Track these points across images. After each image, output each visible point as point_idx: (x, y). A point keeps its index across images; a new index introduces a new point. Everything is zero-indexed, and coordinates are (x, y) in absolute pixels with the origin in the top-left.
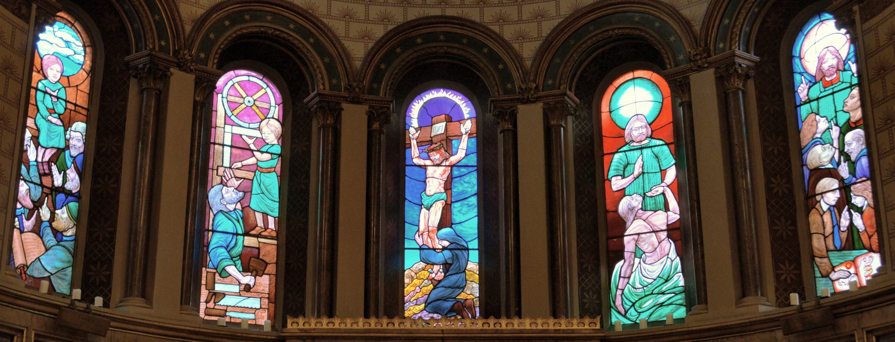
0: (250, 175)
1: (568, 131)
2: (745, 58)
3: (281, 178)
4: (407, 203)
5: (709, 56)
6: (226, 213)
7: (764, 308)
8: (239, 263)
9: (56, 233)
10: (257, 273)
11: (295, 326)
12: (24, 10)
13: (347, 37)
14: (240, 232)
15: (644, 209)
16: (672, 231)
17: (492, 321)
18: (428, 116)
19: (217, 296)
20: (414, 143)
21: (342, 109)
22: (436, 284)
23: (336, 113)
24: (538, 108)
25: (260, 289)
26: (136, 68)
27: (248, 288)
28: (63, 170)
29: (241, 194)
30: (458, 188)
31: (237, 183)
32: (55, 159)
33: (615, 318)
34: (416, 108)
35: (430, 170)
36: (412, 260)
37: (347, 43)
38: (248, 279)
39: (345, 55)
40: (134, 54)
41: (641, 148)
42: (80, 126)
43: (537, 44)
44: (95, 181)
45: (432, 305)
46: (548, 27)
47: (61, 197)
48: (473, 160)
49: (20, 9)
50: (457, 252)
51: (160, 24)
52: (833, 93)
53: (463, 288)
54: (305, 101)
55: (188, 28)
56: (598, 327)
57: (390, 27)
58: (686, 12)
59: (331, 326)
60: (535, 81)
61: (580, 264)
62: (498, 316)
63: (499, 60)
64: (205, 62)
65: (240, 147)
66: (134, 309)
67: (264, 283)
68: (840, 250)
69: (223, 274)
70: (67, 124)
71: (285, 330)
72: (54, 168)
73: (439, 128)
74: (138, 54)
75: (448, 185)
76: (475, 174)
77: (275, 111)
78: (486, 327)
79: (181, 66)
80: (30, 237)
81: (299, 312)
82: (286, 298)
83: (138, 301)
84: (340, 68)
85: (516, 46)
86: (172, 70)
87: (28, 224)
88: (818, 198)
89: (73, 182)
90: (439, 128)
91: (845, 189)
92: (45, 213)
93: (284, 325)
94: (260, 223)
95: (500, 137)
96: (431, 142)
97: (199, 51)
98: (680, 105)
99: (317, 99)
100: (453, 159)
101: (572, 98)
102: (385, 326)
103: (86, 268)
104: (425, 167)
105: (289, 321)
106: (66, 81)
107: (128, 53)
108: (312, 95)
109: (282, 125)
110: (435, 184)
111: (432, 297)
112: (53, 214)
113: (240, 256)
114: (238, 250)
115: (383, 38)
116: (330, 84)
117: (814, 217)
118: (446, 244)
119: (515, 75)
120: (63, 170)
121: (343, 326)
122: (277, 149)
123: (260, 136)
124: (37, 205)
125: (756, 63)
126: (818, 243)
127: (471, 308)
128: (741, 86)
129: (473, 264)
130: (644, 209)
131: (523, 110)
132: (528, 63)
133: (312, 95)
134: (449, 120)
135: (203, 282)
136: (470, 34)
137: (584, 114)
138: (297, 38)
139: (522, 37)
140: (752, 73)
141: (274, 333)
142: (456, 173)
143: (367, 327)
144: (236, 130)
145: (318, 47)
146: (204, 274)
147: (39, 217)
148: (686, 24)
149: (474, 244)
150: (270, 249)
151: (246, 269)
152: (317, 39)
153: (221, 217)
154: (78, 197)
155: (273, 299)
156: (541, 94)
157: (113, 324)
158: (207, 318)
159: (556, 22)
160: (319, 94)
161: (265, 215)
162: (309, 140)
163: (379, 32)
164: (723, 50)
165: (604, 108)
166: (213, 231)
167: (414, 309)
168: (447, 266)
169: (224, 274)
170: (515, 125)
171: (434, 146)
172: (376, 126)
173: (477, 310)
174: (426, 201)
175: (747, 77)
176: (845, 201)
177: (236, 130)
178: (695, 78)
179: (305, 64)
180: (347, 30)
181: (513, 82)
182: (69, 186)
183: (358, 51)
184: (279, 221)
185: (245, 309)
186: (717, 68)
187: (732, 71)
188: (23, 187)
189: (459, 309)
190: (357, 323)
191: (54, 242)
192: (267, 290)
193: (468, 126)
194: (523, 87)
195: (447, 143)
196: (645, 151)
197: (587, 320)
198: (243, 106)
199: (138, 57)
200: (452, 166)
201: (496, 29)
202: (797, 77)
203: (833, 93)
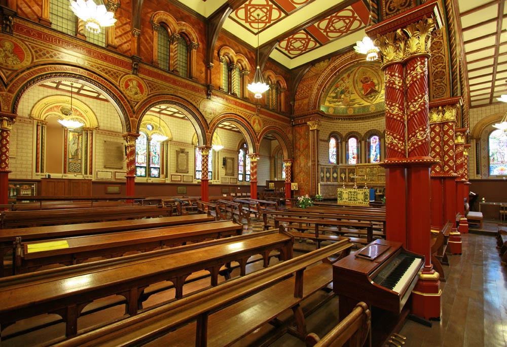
89: (335, 153)
90: (374, 141)
129: (378, 156)
193: (378, 140)
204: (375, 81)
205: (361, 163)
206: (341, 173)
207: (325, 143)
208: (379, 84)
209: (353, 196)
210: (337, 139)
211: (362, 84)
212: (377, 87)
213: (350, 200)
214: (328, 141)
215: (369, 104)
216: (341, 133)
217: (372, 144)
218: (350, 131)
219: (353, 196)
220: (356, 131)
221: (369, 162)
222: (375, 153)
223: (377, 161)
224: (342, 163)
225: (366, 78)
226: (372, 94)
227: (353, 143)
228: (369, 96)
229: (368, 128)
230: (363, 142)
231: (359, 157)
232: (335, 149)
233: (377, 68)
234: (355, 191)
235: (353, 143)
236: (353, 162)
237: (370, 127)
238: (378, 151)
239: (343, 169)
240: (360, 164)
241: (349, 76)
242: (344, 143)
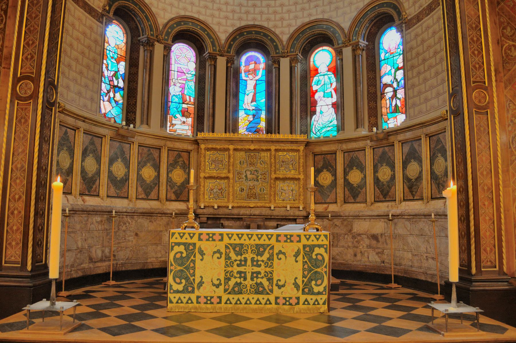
0: (184, 82)
1: (298, 68)
2: (363, 43)
3: (195, 83)
4: (240, 93)
5: (350, 42)
6: (176, 96)
7: (364, 132)
8: (181, 113)
9: (116, 102)
10: (187, 117)
11: (201, 136)
12: (101, 20)
13: (219, 32)
14: (181, 102)
15: (324, 97)
16: (334, 105)
17: (269, 135)
18: (248, 62)
19: (172, 125)
20: (243, 72)
21: (217, 58)
22: (250, 122)
23: (215, 60)
24: (288, 59)
25: (188, 123)
26: (142, 42)
27: (184, 122)
28: (117, 79)
29: (181, 89)
30: (258, 87)
31: (179, 85)
32: (114, 75)
33: (312, 135)
34: (244, 58)
35: (249, 82)
36: (241, 114)
37: (219, 34)
38: (184, 119)
39: (218, 38)
40: (141, 37)
41: (324, 75)
42: (123, 63)
43: (288, 36)
44: (129, 83)
45: (248, 129)
46: (292, 29)
47: (117, 89)
48: (264, 78)
49: (99, 19)
50: (258, 111)
51: (150, 26)
52: (393, 57)
53: (259, 124)
54: (204, 55)
55: (161, 27)
56: (306, 138)
57: (235, 28)
58: (343, 25)
59: (213, 136)
60: (287, 49)
61: (301, 116)
62: (271, 133)
63: (274, 41)
64: (167, 40)
65: (181, 72)
66: (144, 129)
67: (190, 120)
68: (392, 113)
69: (175, 117)
70: (118, 62)
71: (197, 137)
72: (114, 78)
73: (252, 66)
74: (143, 37)
75: (255, 88)
76: (264, 83)
77: (193, 59)
78: (267, 137)
79: (158, 41)
80: (107, 103)
81: (202, 131)
82: (197, 126)
83: (146, 126)
84: (216, 44)
85: (280, 36)
86: (155, 43)
87: (106, 99)
88: (385, 94)
89: (121, 84)
90: (252, 66)
91: (395, 91)
92: (112, 95)
93: (197, 135)
94: (188, 99)
95: (274, 70)
96: (249, 71)
97: (165, 35)
98: (339, 59)
99: (208, 55)
100: (257, 78)
101: (300, 56)
102: (232, 136)
103: (127, 115)
104: (246, 80)
105: (199, 134)
106: (117, 47)
107: (139, 36)
108: (206, 53)
109: (196, 64)
111: (249, 127)
112: (114, 95)
113: (181, 111)
114: (180, 109)
115: (232, 32)
116: (213, 49)
117: (383, 101)
118: (254, 108)
119: (280, 47)
120: (117, 79)
121: (217, 136)
122: (194, 73)
123: (187, 68)
124: (109, 92)
125: (367, 45)
126: (384, 110)
127: (262, 131)
128: (361, 53)
130: (324, 97)
131: (282, 60)
132: (285, 43)
133: (206, 53)
134: (256, 63)
135: (168, 120)
136: (264, 31)
137: (304, 62)
138: (201, 32)
139: (282, 33)
140: (365, 48)
141: (193, 138)
142: (258, 82)
143: (226, 136)
144: (179, 66)
145: (208, 35)
146: (168, 117)
147: (109, 96)
148: (342, 29)
149: (264, 108)
150: (192, 108)
151: (183, 115)
152: (208, 32)
153: (174, 97)
154: (123, 89)
155: (193, 127)
156: (289, 54)
157: (137, 134)
158: (170, 132)
159: (295, 28)
160: (209, 53)
161: (190, 97)
162: (205, 70)
163: (231, 30)
164: (355, 39)
165: (312, 60)
166: (171, 102)
167: (242, 130)
168: (254, 116)
169: (175, 117)
170: (279, 66)
171: (250, 73)
172: (229, 65)
173: (264, 131)
174: (247, 93)
175: (363, 50)
176: (395, 96)
177: (179, 66)
178: (344, 50)
179: (204, 41)
180: (219, 29)
181: (279, 50)
182: (119, 85)
184: (195, 99)
185: (183, 130)
186: (353, 46)
187: (358, 47)
188: (103, 85)
189: (257, 131)
190: (222, 135)
191: (115, 105)
192: (191, 123)
193: (262, 66)
194: (283, 51)
195: (255, 71)
196: (325, 76)
197: (302, 135)
198: (181, 57)
199: (143, 38)
200: (256, 80)
201: (273, 29)
202: (381, 51)
203: (393, 57)
206: (141, 165)
209: (249, 269)
213: (238, 289)
216: (154, 10)
217: (243, 75)
218: (182, 13)
219: (249, 269)
220: (202, 18)
222: (251, 107)
229: (240, 19)
230: (221, 62)
232: (122, 67)
234: (264, 241)
237: (244, 16)
239: (149, 147)
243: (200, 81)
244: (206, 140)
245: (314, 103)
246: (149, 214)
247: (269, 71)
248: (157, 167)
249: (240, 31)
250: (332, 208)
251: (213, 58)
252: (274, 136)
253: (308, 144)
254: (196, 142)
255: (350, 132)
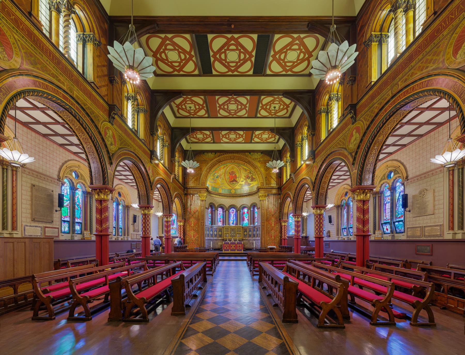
7: (252, 225)
36: (231, 221)
45: (232, 224)
65: (220, 214)
66: (214, 226)
110: (232, 215)
167: (231, 224)
183: (227, 207)
195: (233, 212)
199: (214, 209)
204: (237, 175)
205: (226, 225)
207: (206, 210)
208: (239, 177)
210: (212, 208)
211: (229, 175)
212: (237, 179)
214: (208, 209)
215: (231, 188)
221: (230, 225)
223: (234, 224)
224: (215, 224)
225: (233, 172)
226: (234, 182)
227: (220, 211)
228: (232, 183)
230: (227, 212)
231: (224, 222)
233: (241, 168)
235: (220, 211)
236: (220, 224)
238: (235, 218)
240: (225, 226)
241: (224, 168)
242: (216, 211)
243: (223, 215)
244: (225, 227)
245: (244, 219)
246: (216, 240)
247: (236, 213)
248: (217, 232)
249: (230, 206)
250: (247, 238)
251: (225, 211)
252: (237, 226)
253: (242, 227)
254: (223, 227)
255: (249, 226)
